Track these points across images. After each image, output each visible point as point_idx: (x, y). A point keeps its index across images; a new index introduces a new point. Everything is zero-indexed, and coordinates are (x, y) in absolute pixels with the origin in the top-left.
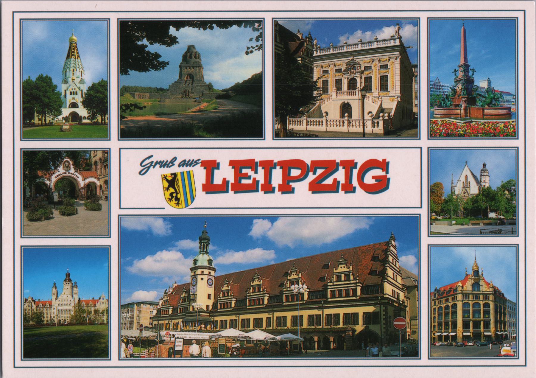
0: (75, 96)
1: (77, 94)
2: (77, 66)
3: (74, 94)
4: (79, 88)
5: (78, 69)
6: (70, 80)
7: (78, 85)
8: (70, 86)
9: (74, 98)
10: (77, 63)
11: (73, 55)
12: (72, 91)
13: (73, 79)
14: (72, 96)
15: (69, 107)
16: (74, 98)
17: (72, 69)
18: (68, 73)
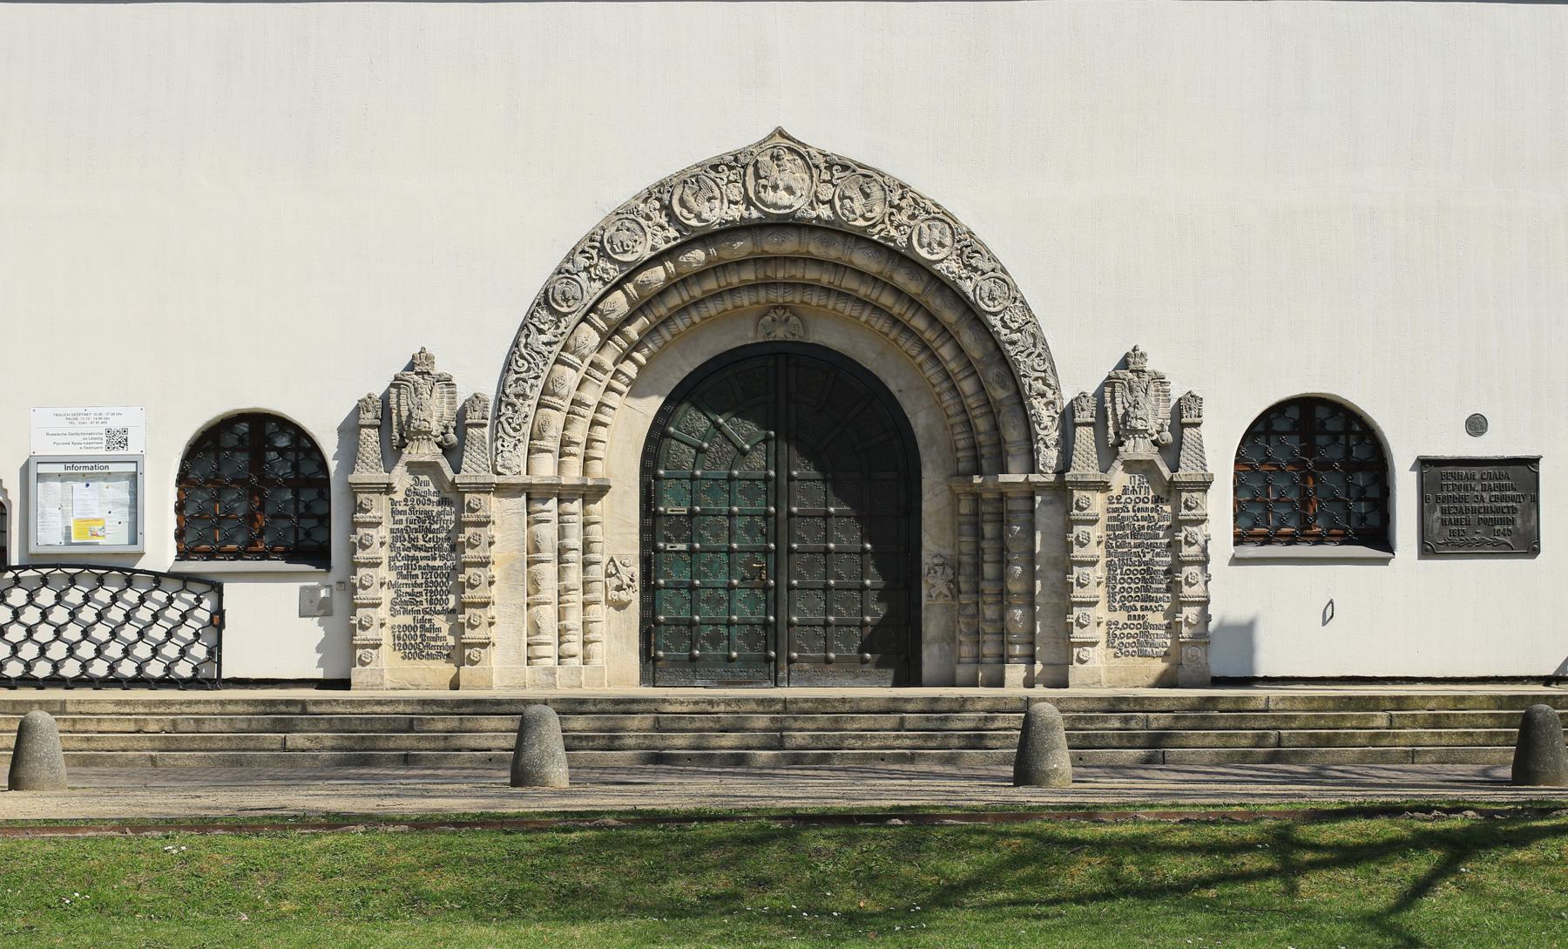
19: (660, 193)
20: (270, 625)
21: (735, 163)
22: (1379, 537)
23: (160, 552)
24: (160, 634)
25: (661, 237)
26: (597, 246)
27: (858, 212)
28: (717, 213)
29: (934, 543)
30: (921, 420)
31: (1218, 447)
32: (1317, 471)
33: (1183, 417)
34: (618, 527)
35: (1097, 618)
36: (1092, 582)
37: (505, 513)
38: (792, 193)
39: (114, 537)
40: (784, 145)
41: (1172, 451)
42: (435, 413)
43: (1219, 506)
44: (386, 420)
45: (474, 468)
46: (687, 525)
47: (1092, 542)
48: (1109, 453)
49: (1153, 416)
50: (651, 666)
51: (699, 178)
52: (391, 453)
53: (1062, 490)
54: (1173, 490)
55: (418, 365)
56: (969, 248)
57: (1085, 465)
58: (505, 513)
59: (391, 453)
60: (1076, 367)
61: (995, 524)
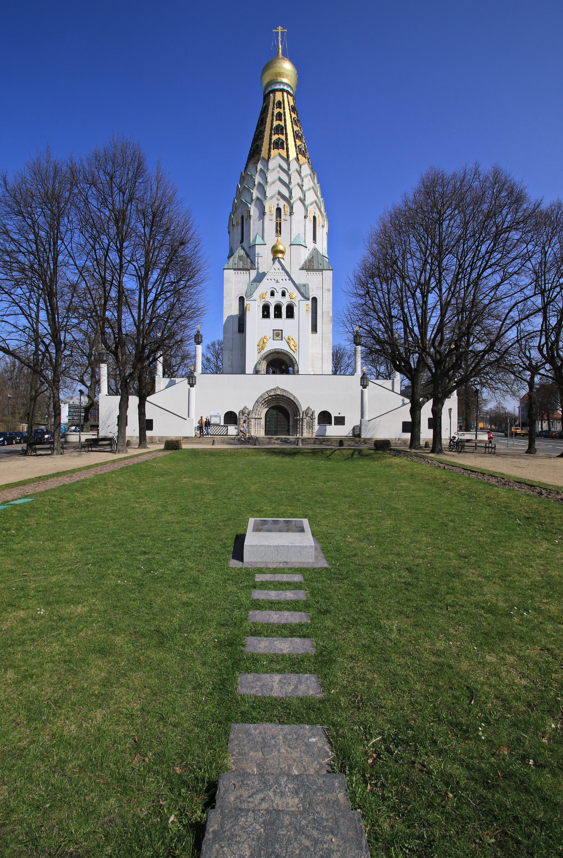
0: (283, 323)
1: (290, 313)
2: (297, 193)
3: (278, 315)
4: (302, 290)
5: (298, 207)
6: (263, 254)
7: (301, 277)
8: (260, 278)
9: (278, 334)
10: (295, 179)
11: (280, 145)
12: (273, 302)
13: (275, 251)
14: (273, 323)
15: (257, 372)
16: (278, 334)
17: (270, 206)
18: (254, 224)
19: (267, 392)
20: (232, 430)
21: (274, 389)
22: (331, 423)
23: (222, 424)
24: (222, 431)
25: (267, 396)
26: (261, 397)
27: (284, 394)
28: (272, 394)
29: (291, 423)
30: (290, 412)
31: (316, 415)
32: (325, 418)
33: (313, 413)
34: (263, 421)
35: (305, 430)
36: (305, 427)
37: (253, 420)
38: (279, 392)
39: (218, 422)
40: (278, 388)
41: (312, 415)
42: (247, 412)
43: (316, 421)
44: (242, 412)
45: (250, 416)
46: (269, 422)
47: (305, 423)
48: (307, 416)
49: (310, 413)
50: (266, 434)
51: (270, 391)
52: (243, 415)
53: (302, 419)
54: (312, 418)
55: (245, 407)
56: (294, 397)
57: (304, 417)
58: (253, 420)
59: (243, 415)
60: (303, 408)
61: (296, 422)
